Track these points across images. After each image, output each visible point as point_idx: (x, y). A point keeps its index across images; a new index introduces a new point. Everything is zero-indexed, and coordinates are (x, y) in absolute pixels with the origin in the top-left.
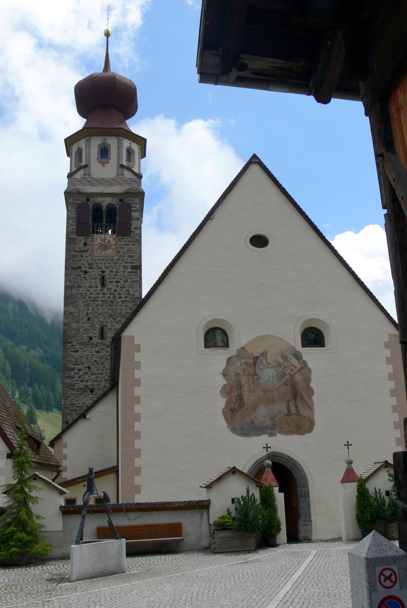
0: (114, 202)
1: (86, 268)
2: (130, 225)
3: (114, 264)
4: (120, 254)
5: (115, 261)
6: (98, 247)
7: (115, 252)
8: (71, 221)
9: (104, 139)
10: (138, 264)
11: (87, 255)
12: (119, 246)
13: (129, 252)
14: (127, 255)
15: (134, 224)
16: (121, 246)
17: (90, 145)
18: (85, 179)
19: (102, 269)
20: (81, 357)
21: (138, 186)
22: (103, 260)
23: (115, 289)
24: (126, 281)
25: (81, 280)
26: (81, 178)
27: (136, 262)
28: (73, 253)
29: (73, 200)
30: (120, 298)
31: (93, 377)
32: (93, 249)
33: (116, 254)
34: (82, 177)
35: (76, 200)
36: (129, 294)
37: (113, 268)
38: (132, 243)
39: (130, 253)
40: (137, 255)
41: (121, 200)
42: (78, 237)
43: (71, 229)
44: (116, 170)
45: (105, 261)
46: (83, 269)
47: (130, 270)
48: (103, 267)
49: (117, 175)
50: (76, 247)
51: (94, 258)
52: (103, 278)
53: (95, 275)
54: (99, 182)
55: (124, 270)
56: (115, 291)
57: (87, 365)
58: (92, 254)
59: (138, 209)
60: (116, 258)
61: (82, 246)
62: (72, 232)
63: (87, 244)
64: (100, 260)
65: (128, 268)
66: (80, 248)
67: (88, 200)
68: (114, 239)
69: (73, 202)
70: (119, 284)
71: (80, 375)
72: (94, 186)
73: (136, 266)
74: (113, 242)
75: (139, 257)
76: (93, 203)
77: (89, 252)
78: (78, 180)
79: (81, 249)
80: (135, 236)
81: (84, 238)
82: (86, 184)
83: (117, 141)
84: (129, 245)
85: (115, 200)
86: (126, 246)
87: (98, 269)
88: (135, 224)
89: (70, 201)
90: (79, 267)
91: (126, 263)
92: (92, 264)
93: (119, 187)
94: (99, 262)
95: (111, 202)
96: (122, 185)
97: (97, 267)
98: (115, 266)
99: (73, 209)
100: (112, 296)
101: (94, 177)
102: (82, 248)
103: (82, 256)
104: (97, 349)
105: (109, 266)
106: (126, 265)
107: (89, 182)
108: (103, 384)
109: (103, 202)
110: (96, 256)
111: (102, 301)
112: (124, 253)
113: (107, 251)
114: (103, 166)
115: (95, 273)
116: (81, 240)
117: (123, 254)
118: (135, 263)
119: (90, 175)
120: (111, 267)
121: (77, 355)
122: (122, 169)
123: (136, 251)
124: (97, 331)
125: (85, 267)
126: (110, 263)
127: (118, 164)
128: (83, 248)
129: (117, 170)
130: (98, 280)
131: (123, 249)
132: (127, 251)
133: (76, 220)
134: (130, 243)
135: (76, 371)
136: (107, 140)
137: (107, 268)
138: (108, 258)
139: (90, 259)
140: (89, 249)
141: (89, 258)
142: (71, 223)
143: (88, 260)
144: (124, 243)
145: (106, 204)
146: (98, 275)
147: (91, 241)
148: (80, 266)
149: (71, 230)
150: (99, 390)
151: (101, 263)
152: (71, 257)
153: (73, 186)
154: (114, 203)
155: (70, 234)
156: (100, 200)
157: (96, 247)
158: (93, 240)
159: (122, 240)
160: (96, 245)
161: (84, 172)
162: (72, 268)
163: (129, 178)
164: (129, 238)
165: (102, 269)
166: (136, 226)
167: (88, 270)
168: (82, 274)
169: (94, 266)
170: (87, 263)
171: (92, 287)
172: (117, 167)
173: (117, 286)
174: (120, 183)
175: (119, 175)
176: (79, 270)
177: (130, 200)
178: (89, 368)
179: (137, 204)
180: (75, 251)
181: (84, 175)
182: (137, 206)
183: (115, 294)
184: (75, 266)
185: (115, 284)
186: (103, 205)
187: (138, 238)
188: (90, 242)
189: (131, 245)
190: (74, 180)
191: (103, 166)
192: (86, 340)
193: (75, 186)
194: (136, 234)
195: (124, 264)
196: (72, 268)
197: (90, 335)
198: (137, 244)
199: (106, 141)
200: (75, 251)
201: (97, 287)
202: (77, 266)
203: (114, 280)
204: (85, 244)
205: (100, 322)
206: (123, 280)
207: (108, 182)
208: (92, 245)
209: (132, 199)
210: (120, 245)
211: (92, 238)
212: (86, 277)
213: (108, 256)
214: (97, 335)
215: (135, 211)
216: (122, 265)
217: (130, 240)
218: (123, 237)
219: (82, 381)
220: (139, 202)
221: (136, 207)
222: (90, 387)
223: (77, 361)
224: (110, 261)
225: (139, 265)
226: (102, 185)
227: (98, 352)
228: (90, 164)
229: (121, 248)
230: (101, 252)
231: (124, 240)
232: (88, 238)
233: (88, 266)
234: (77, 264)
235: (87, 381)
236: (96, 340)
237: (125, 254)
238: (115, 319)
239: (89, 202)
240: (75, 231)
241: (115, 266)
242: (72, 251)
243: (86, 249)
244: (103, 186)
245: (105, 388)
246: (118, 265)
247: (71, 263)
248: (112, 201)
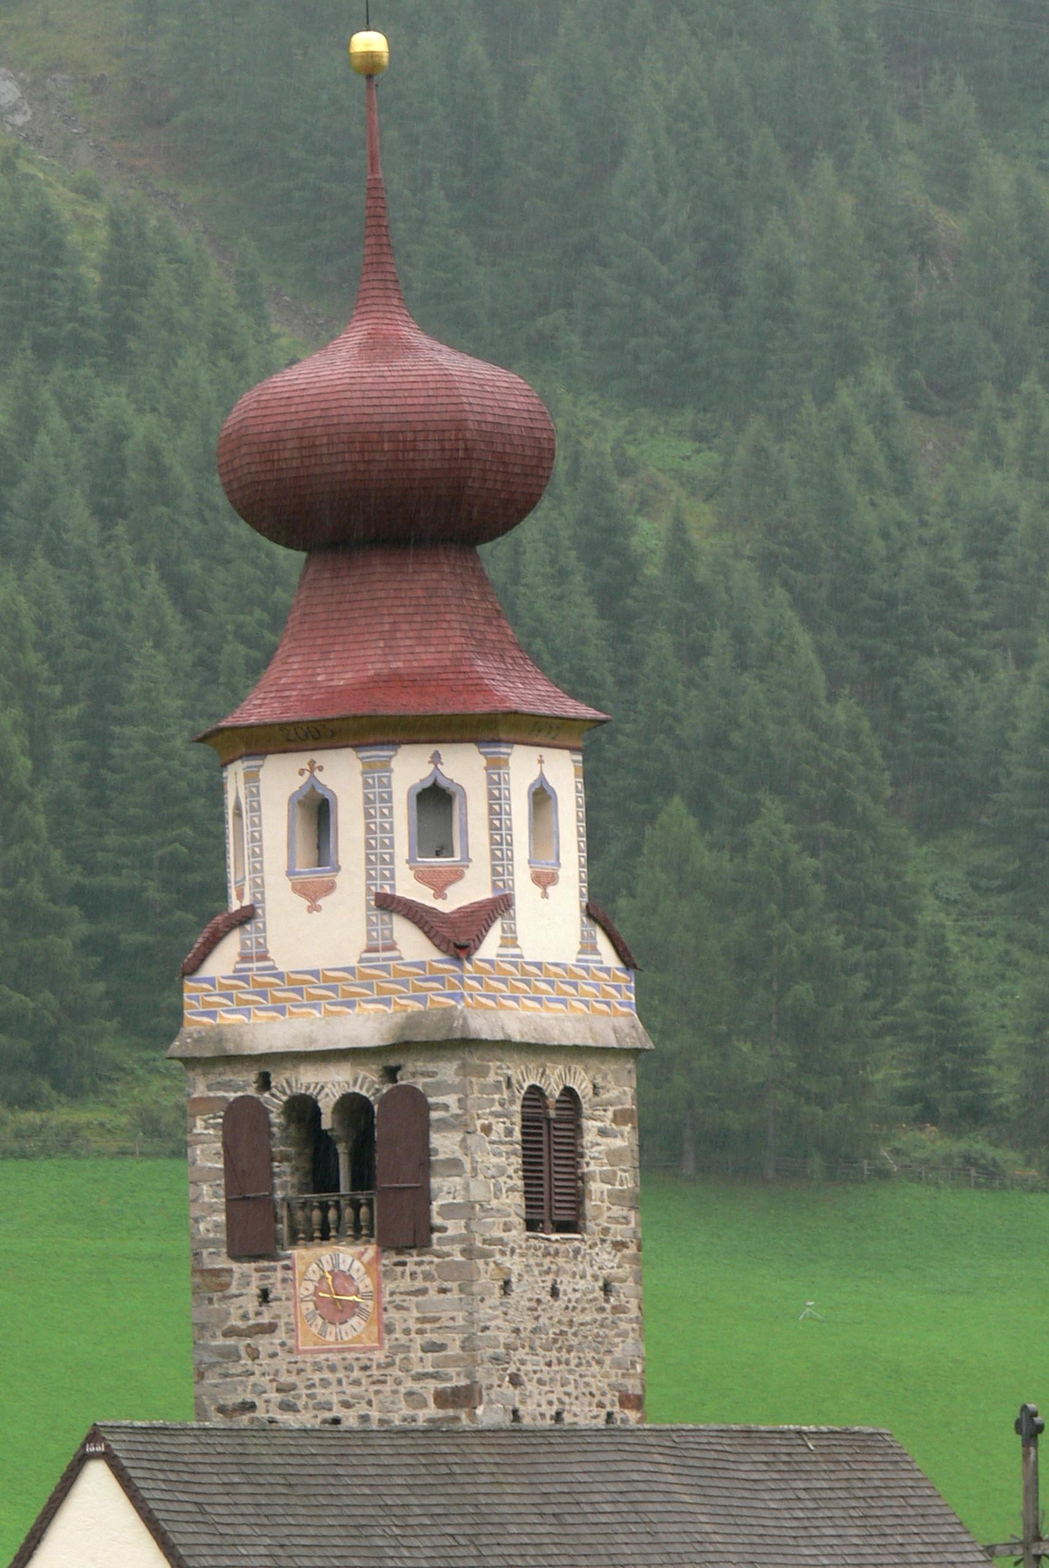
0: (361, 1087)
1: (272, 1407)
2: (425, 1196)
3: (374, 1383)
4: (393, 1336)
5: (376, 1372)
6: (311, 1306)
7: (375, 1329)
8: (205, 1187)
9: (312, 764)
10: (463, 1382)
11: (271, 1350)
12: (387, 1298)
13: (428, 1326)
14: (419, 1340)
15: (440, 1190)
16: (397, 1298)
17: (259, 803)
18: (245, 979)
19: (330, 1410)
21: (453, 1003)
22: (333, 1369)
26: (232, 974)
27: (452, 1371)
28: (220, 1341)
29: (210, 1088)
32: (292, 1320)
33: (380, 1340)
34: (236, 971)
35: (222, 1086)
37: (370, 1403)
38: (436, 1284)
39: (432, 1331)
40: (458, 1338)
41: (391, 1074)
42: (234, 1266)
43: (210, 1227)
44: (363, 927)
45: (341, 1374)
48: (335, 1399)
49: (368, 951)
50: (232, 1310)
51: (299, 1358)
54: (299, 992)
55: (412, 1412)
58: (291, 1342)
59: (457, 1116)
60: (379, 1356)
61: (251, 1305)
62: (213, 1242)
63: (271, 1296)
64: (320, 1369)
65: (424, 1404)
66: (245, 1317)
67: (265, 1083)
68: (368, 1266)
69: (209, 1098)
72: (282, 1011)
73: (456, 1391)
74: (365, 1283)
75: (463, 1348)
76: (284, 1098)
77: (281, 1335)
78: (222, 986)
79: (251, 1322)
80: (446, 1249)
81: (257, 1270)
82: (254, 1002)
83: (363, 773)
84: (423, 1292)
85: (365, 1078)
86: (413, 1298)
87: (316, 1412)
88: (445, 1189)
89: (195, 1095)
90: (244, 1403)
91: (419, 1377)
92: (293, 1387)
93: (377, 1012)
94: (316, 1377)
95: (351, 1090)
96: (387, 1002)
97: (311, 1403)
98: (377, 1392)
99: (211, 1131)
101: (282, 968)
102: (251, 1315)
103: (254, 1355)
105: (354, 1397)
106: (417, 1386)
107: (263, 995)
109: (323, 1088)
110: (306, 1352)
112: (407, 1331)
113: (343, 1327)
114: (314, 908)
116: (245, 1281)
117: (403, 1339)
118: (451, 1379)
119: (263, 957)
120: (362, 1398)
122: (386, 918)
123: (453, 1319)
125: (267, 1401)
126: (357, 1383)
127: (368, 889)
128: (258, 1314)
129: (369, 922)
131: (405, 1314)
132: (418, 1320)
133: (222, 1182)
134: (428, 1284)
136: (321, 769)
137: (346, 1405)
138: (350, 1356)
139: (285, 1367)
140: (278, 1317)
141: (282, 1362)
142: (206, 1199)
143: (277, 1373)
144: (405, 1284)
147: (284, 1280)
148: (249, 1397)
149: (208, 1230)
151: (325, 1383)
152: (215, 1359)
153: (206, 1020)
154: (364, 1093)
155: (205, 1253)
156: (307, 1079)
157: (304, 1306)
158: (289, 1274)
159: (399, 1269)
160: (302, 1301)
161: (243, 944)
162: (221, 1410)
163: (417, 959)
164: (427, 1258)
165: (330, 1410)
166: (449, 1200)
169: (299, 1397)
170: (275, 1384)
172: (368, 908)
174: (381, 990)
175: (376, 950)
177: (425, 1074)
179: (450, 1089)
181: (245, 958)
182: (451, 1100)
184: (233, 1399)
186: (320, 1105)
187: (459, 1258)
188: (279, 1286)
189: (432, 1293)
190: (206, 986)
191: (314, 908)
193: (212, 1015)
194: (452, 1240)
195: (409, 1385)
196: (221, 1410)
198: (453, 1285)
199: (317, 773)
202: (240, 1400)
204: (264, 1296)
207: (334, 989)
208: (288, 1299)
209: (431, 1067)
210: (392, 1294)
211: (286, 1268)
213: (350, 1350)
215: (445, 1125)
216: (402, 1390)
217: (426, 1268)
218: (402, 1258)
220: (457, 1080)
221: (446, 1107)
224: (356, 1374)
225: (467, 1387)
226: (314, 1006)
228: (263, 901)
229: (399, 1308)
230: (323, 1333)
231: (408, 1269)
232: (274, 1269)
233: (276, 1397)
234: (240, 1389)
237: (413, 1335)
239: (267, 1095)
240: (222, 1236)
241: (377, 1392)
242: (219, 1333)
243: (265, 1319)
244: (315, 1012)
246: (387, 1388)
247: (216, 1386)
248: (355, 1081)
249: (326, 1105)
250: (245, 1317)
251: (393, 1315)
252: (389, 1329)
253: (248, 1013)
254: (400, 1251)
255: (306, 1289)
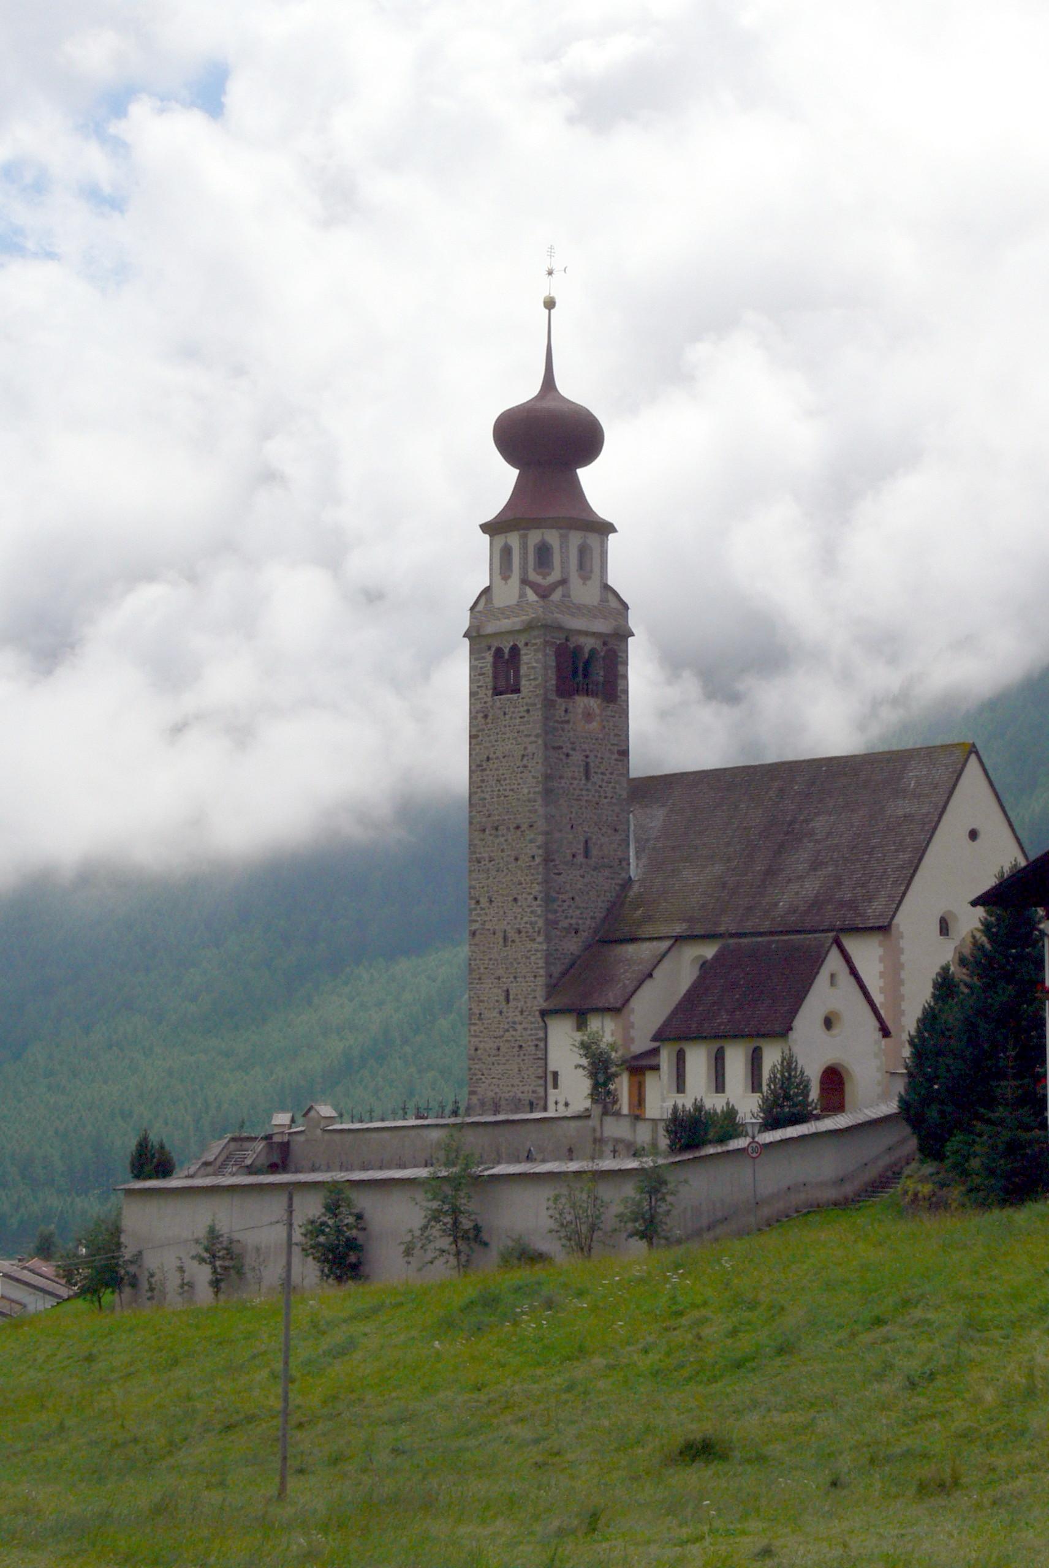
5: (600, 741)
10: (625, 748)
20: (564, 883)
22: (587, 738)
23: (600, 784)
24: (611, 774)
25: (563, 767)
30: (606, 797)
31: (578, 912)
36: (615, 793)
37: (598, 751)
41: (605, 644)
46: (564, 750)
47: (616, 756)
52: (587, 764)
53: (578, 760)
56: (600, 787)
57: (571, 895)
61: (563, 713)
70: (604, 777)
71: (564, 908)
74: (597, 711)
81: (564, 702)
91: (613, 745)
94: (582, 740)
100: (597, 794)
101: (575, 601)
103: (563, 730)
104: (582, 872)
106: (612, 747)
108: (588, 922)
111: (586, 801)
115: (577, 757)
119: (569, 597)
121: (561, 879)
124: (581, 846)
126: (594, 744)
130: (582, 769)
135: (559, 903)
141: (572, 734)
144: (609, 713)
145: (589, 648)
146: (582, 761)
150: (584, 931)
156: (582, 640)
161: (563, 591)
167: (571, 752)
168: (563, 757)
171: (576, 779)
173: (603, 780)
176: (560, 751)
178: (573, 899)
180: (557, 721)
181: (563, 596)
183: (599, 792)
184: (556, 745)
185: (600, 776)
191: (584, 584)
192: (569, 858)
193: (552, 613)
195: (609, 747)
197: (574, 850)
200: (557, 721)
201: (581, 780)
203: (600, 771)
204: (566, 711)
205: (585, 831)
206: (610, 770)
212: (567, 763)
214: (582, 851)
219: (566, 917)
221: (621, 657)
222: (575, 926)
223: (560, 889)
224: (594, 741)
227: (583, 877)
233: (570, 746)
235: (572, 917)
236: (580, 859)
238: (600, 829)
240: (554, 689)
243: (567, 718)
245: (590, 928)
249: (586, 650)
250: (560, 717)
251: (605, 723)
252: (604, 727)
253: (563, 615)
254: (608, 703)
255: (580, 711)
